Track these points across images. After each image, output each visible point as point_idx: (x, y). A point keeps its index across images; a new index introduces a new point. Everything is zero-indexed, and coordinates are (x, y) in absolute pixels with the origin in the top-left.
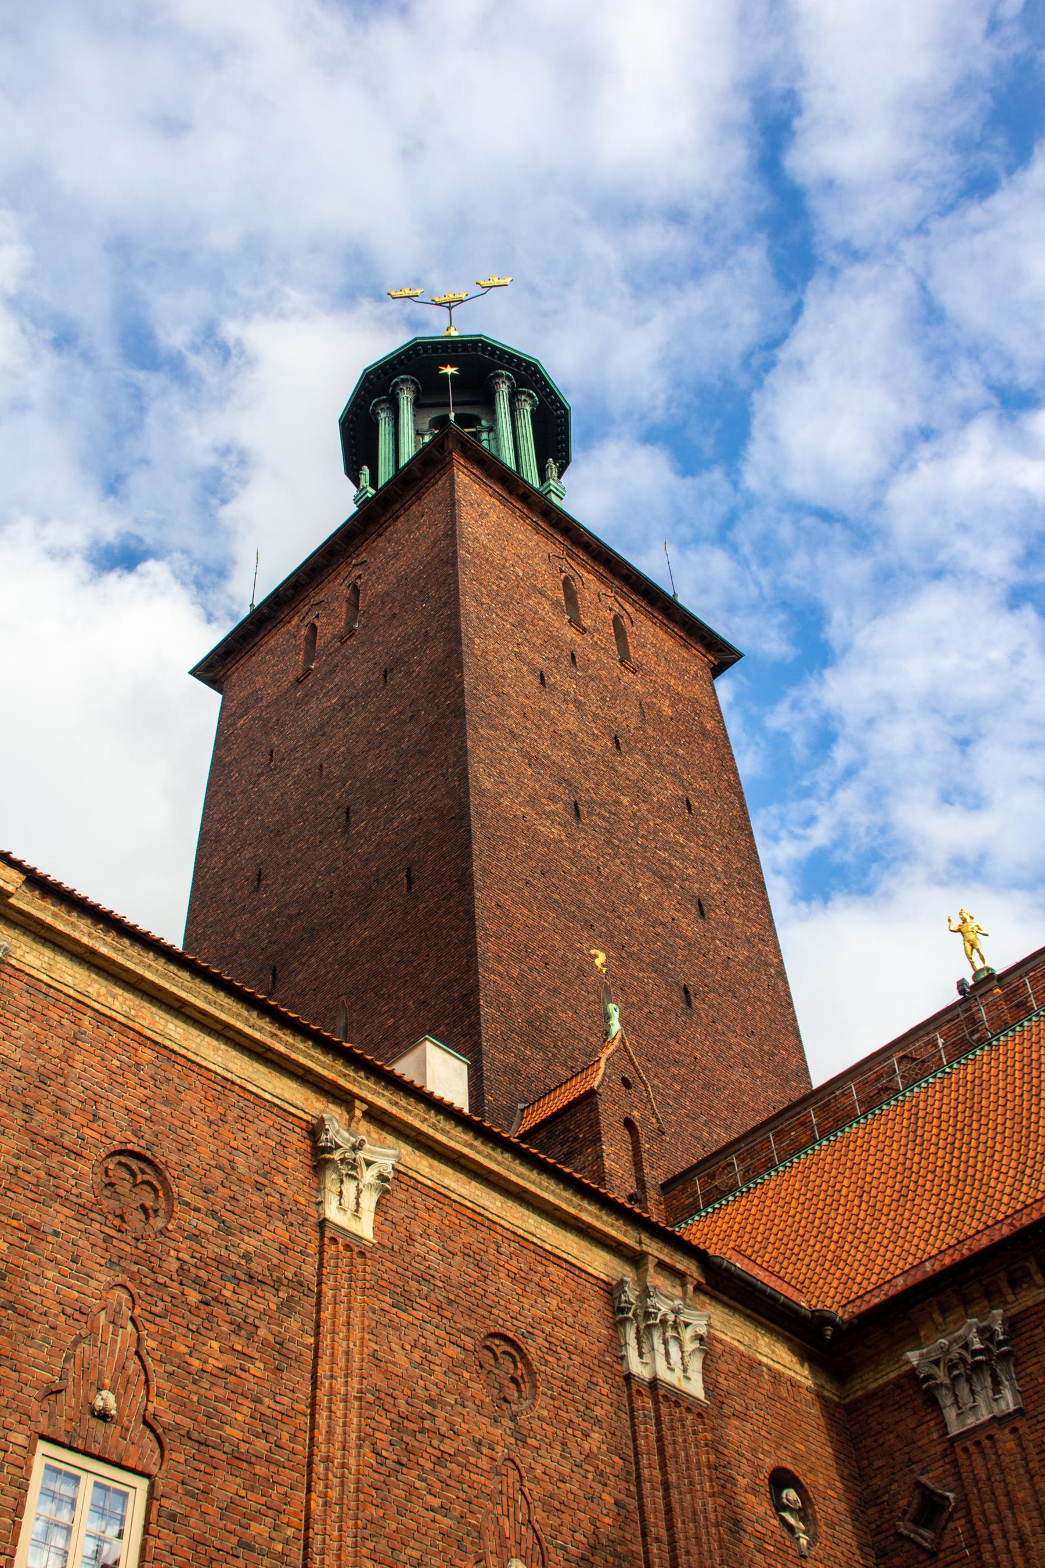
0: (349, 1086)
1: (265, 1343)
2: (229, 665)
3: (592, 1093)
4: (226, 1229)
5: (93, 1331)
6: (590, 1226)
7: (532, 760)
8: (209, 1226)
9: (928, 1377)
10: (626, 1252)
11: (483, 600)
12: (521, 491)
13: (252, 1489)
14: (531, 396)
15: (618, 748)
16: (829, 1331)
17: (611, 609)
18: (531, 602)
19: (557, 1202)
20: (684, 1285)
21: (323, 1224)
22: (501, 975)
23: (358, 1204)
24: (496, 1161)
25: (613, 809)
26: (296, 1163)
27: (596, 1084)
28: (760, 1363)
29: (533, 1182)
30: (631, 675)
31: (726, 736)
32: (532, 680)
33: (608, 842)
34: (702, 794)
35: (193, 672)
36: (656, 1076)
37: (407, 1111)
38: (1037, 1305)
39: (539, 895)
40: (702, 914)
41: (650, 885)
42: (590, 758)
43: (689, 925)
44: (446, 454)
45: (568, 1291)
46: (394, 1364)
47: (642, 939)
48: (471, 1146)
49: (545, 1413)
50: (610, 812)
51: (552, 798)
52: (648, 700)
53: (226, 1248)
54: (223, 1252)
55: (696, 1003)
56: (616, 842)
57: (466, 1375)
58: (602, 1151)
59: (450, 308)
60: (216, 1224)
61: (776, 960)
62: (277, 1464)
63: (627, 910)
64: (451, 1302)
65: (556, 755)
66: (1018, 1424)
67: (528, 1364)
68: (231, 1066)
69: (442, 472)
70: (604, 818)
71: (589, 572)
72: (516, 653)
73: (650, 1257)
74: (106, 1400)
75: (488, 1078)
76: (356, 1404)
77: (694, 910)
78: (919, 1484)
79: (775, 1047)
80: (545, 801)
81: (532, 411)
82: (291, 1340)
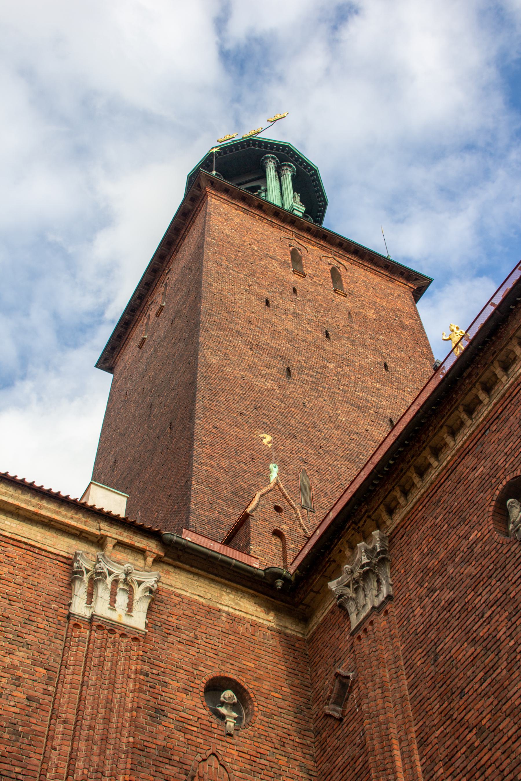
2: (116, 356)
6: (51, 520)
10: (90, 538)
11: (223, 263)
12: (256, 203)
14: (290, 166)
16: (279, 583)
19: (16, 503)
20: (145, 559)
22: (212, 467)
25: (320, 371)
28: (220, 611)
30: (342, 298)
31: (422, 328)
34: (396, 360)
35: (97, 366)
38: (402, 520)
39: (251, 421)
41: (348, 412)
42: (303, 344)
44: (203, 190)
52: (356, 310)
56: (321, 389)
63: (327, 426)
65: (274, 344)
66: (388, 608)
69: (203, 202)
70: (311, 376)
71: (313, 246)
73: (109, 539)
78: (337, 675)
81: (293, 176)
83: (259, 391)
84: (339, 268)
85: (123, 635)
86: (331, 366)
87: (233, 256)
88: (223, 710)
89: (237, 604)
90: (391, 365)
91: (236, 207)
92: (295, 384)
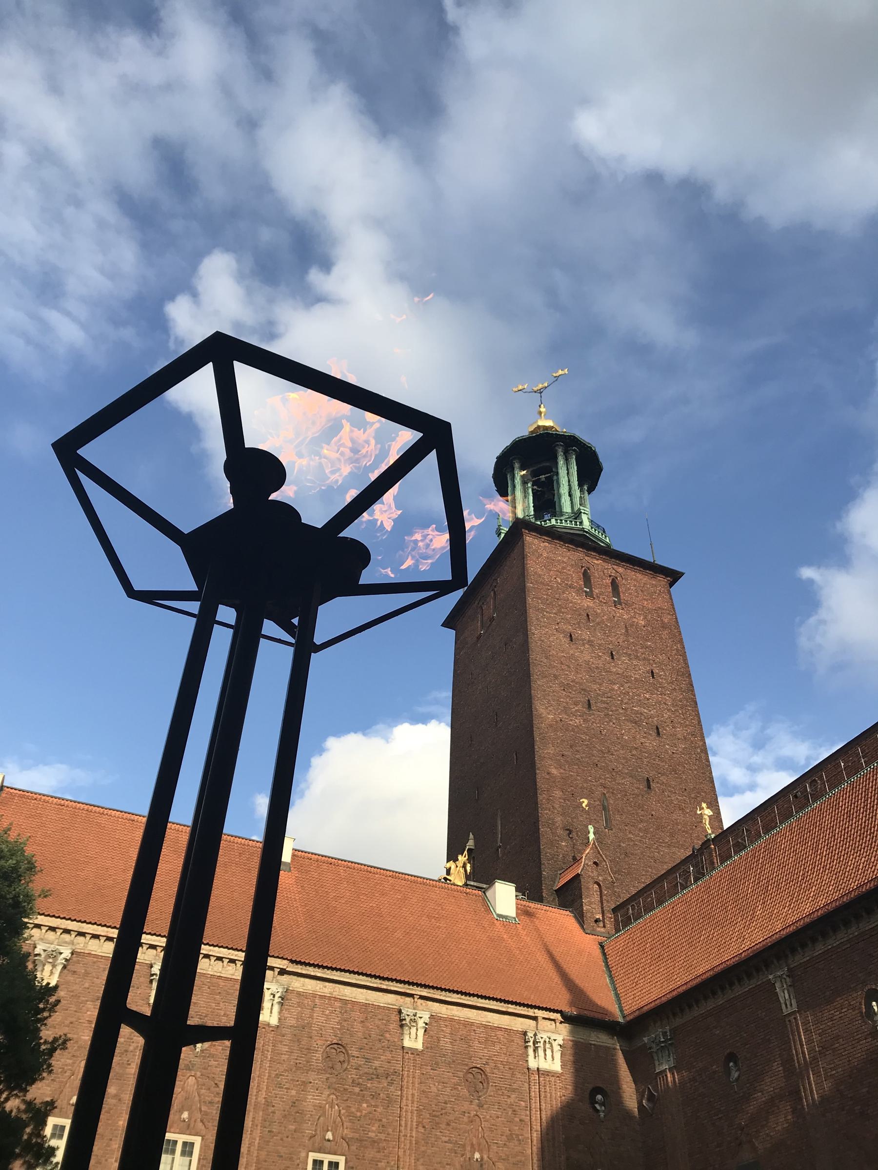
3: (578, 875)
4: (368, 1060)
5: (324, 1113)
7: (565, 687)
9: (650, 1048)
13: (379, 1152)
14: (574, 450)
15: (613, 658)
17: (610, 576)
24: (471, 1001)
25: (609, 695)
26: (394, 1026)
27: (580, 871)
28: (591, 1044)
29: (487, 1004)
30: (621, 611)
32: (565, 641)
33: (607, 715)
35: (442, 625)
36: (630, 832)
37: (434, 994)
40: (658, 733)
43: (651, 743)
45: (504, 1040)
46: (431, 1092)
47: (623, 761)
48: (460, 999)
49: (492, 1094)
50: (608, 697)
51: (576, 704)
53: (369, 1068)
54: (366, 1070)
55: (653, 785)
56: (611, 713)
57: (460, 1088)
58: (582, 902)
59: (541, 393)
61: (701, 743)
63: (616, 748)
64: (454, 1062)
67: (486, 1075)
70: (604, 702)
71: (598, 560)
72: (556, 629)
74: (329, 1136)
75: (544, 864)
76: (416, 1112)
77: (654, 734)
79: (698, 793)
80: (572, 707)
82: (392, 1095)
83: (573, 730)
84: (617, 578)
87: (545, 597)
88: (597, 1106)
89: (598, 1037)
90: (656, 671)
91: (543, 540)
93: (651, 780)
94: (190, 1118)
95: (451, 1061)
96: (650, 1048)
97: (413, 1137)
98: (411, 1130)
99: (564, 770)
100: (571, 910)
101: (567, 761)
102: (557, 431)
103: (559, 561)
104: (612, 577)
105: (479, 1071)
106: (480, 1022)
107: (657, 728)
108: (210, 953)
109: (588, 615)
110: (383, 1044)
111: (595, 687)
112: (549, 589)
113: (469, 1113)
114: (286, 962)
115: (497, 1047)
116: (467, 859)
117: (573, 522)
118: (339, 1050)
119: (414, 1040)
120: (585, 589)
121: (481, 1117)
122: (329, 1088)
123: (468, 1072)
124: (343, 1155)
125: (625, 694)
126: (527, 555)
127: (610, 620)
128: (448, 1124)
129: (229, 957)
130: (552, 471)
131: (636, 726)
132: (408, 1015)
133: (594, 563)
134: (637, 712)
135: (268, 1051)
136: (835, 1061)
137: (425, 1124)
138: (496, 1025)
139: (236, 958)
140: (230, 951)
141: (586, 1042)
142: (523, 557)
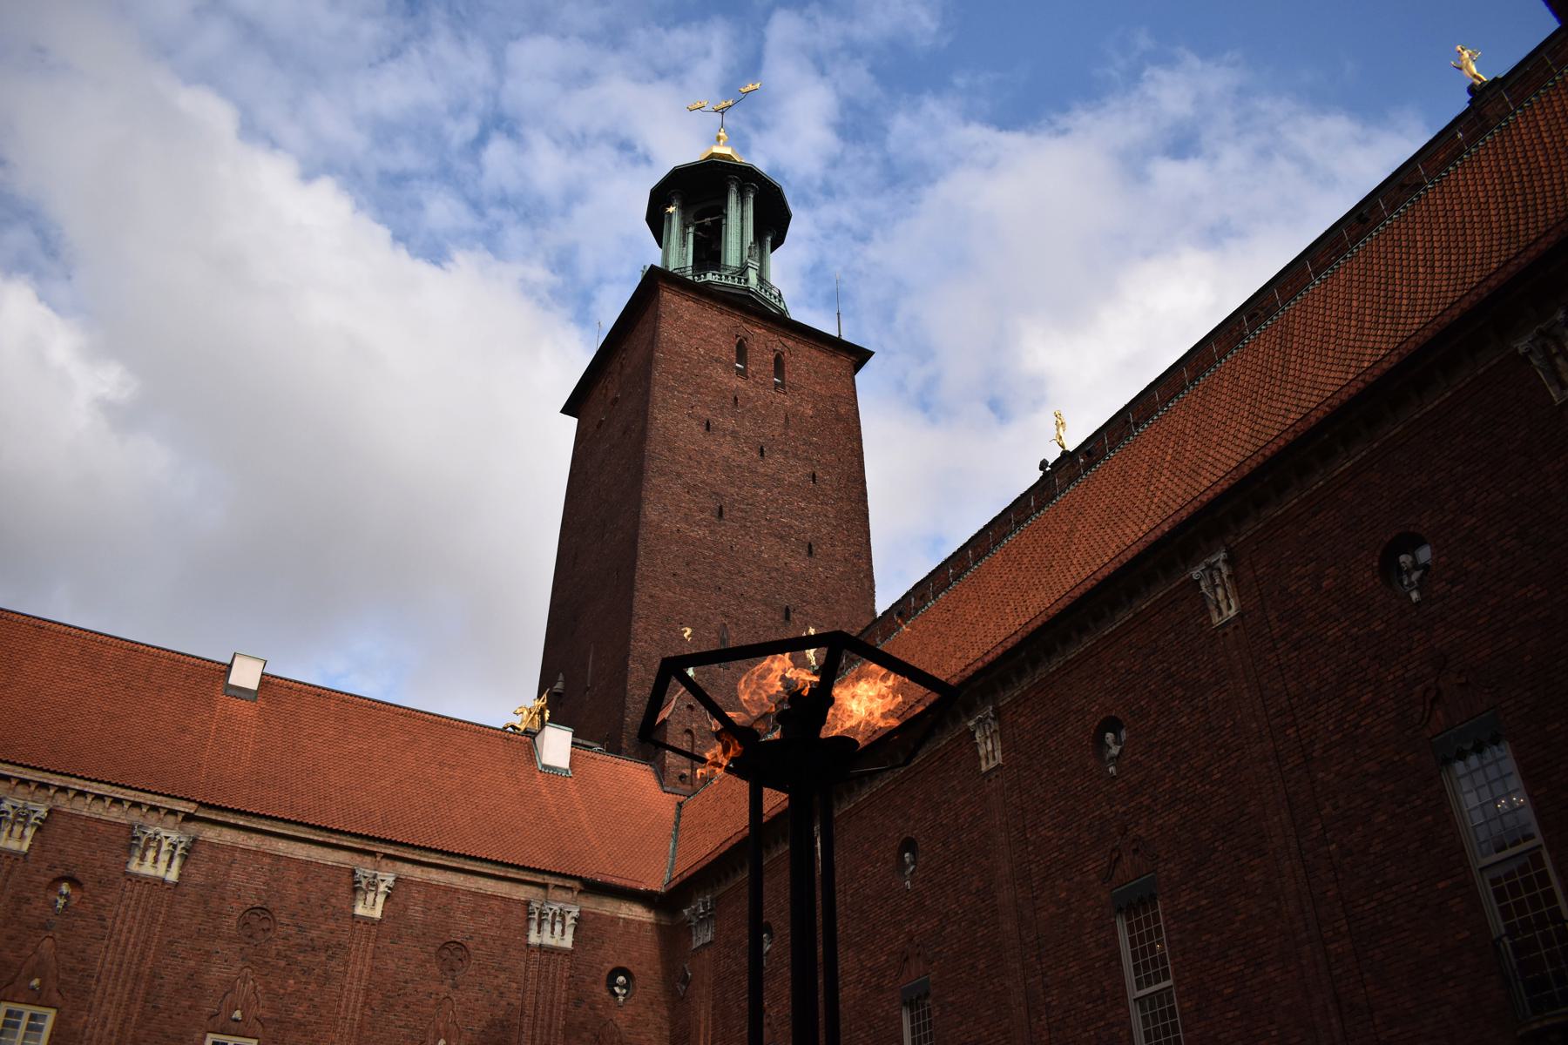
0: (371, 849)
1: (318, 975)
4: (301, 929)
7: (691, 489)
8: (293, 931)
13: (304, 1036)
15: (762, 455)
16: (656, 899)
17: (774, 350)
18: (707, 371)
20: (573, 892)
21: (354, 916)
22: (646, 642)
23: (375, 901)
25: (750, 501)
26: (343, 890)
28: (619, 918)
30: (782, 396)
32: (699, 430)
35: (562, 412)
40: (810, 552)
43: (799, 564)
47: (757, 585)
48: (441, 859)
49: (473, 972)
50: (748, 505)
54: (298, 941)
55: (793, 616)
56: (749, 524)
57: (428, 965)
58: (665, 754)
59: (722, 113)
60: (297, 929)
62: (320, 1023)
64: (424, 934)
67: (468, 952)
68: (312, 854)
70: (742, 511)
74: (237, 1014)
75: (628, 708)
76: (362, 992)
77: (804, 552)
78: (684, 968)
84: (783, 353)
85: (559, 954)
86: (761, 492)
88: (617, 990)
89: (630, 910)
92: (725, 525)
93: (791, 609)
94: (41, 985)
95: (421, 934)
96: (690, 922)
97: (354, 1020)
98: (354, 1011)
99: (674, 593)
100: (653, 763)
101: (678, 582)
102: (736, 161)
103: (705, 326)
104: (776, 352)
105: (459, 946)
106: (467, 889)
107: (810, 546)
108: (86, 789)
109: (736, 399)
110: (326, 911)
111: (733, 490)
112: (686, 362)
113: (437, 994)
114: (193, 805)
115: (488, 919)
116: (546, 704)
117: (736, 279)
118: (262, 916)
119: (371, 907)
120: (737, 365)
121: (455, 999)
122: (243, 959)
123: (443, 947)
124: (254, 1038)
125: (772, 501)
126: (661, 316)
127: (767, 407)
128: (406, 1007)
129: (112, 795)
130: (722, 213)
131: (781, 542)
132: (365, 877)
133: (755, 332)
134: (786, 525)
135: (160, 913)
136: (862, 925)
137: (373, 1006)
138: (489, 893)
139: (122, 797)
140: (114, 788)
141: (613, 915)
142: (657, 318)
